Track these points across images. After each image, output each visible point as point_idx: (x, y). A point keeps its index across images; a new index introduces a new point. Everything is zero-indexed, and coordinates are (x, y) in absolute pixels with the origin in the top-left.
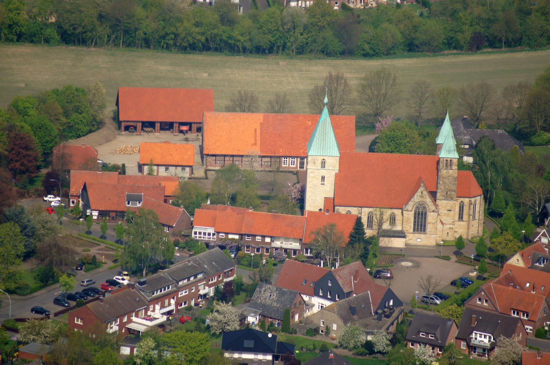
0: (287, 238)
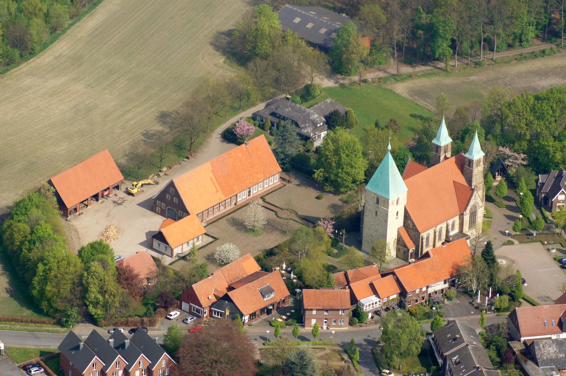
0: (437, 280)
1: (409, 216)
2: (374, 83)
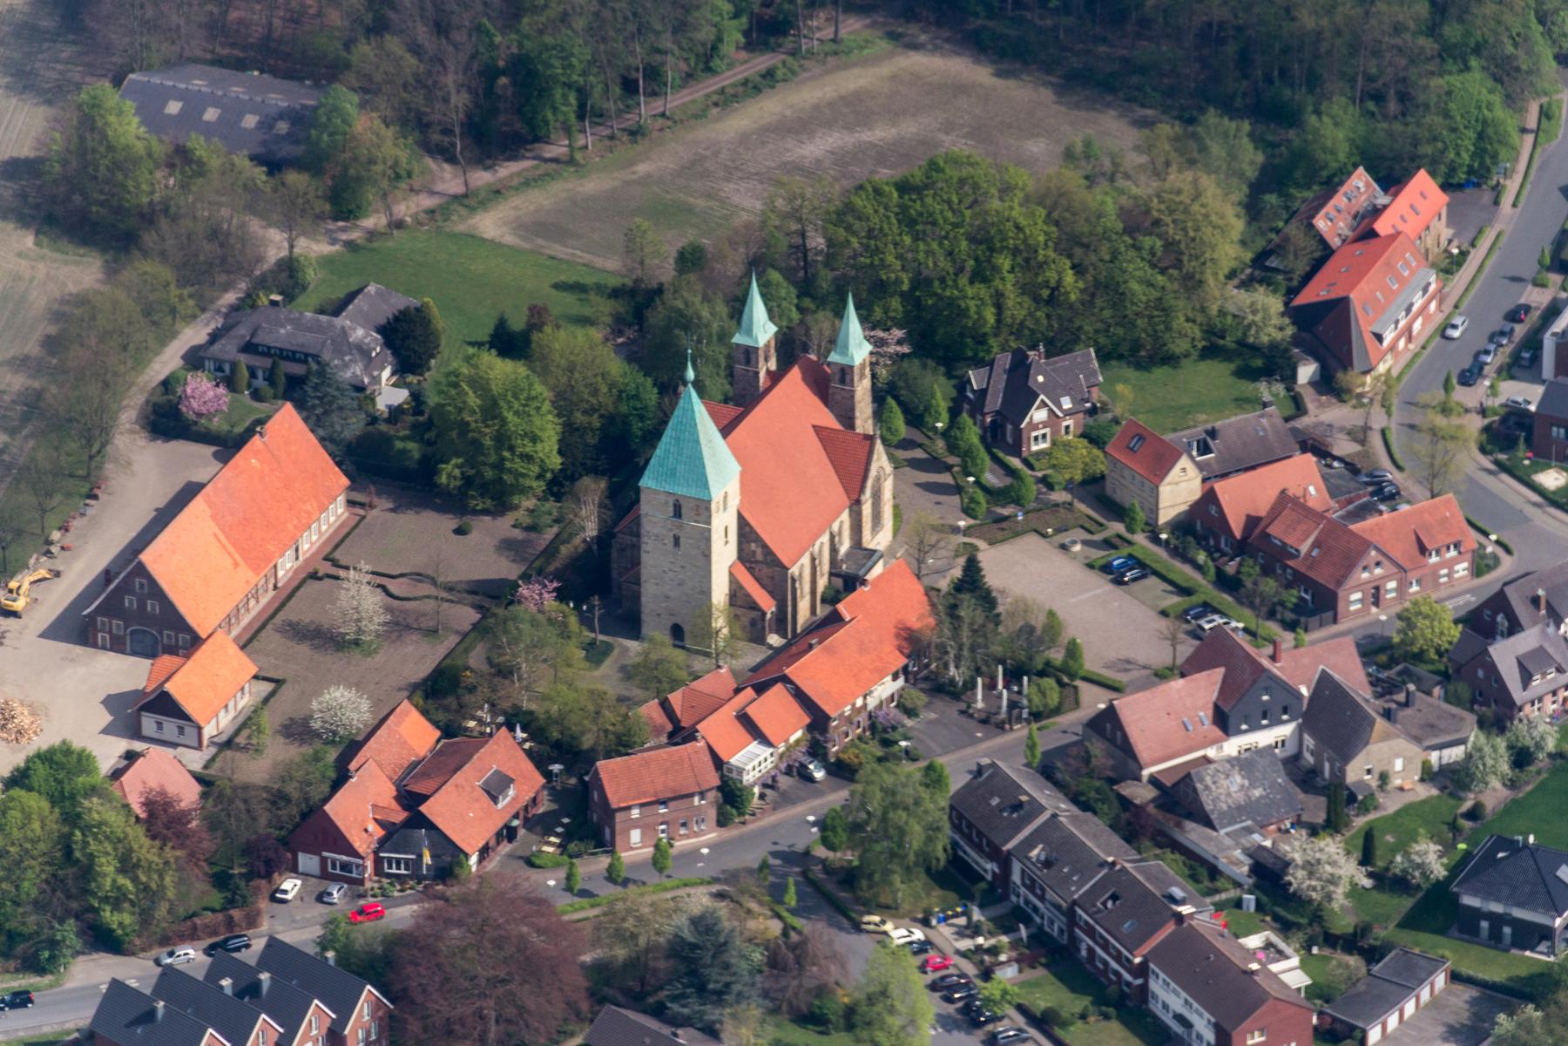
1: (752, 530)
2: (421, 224)
